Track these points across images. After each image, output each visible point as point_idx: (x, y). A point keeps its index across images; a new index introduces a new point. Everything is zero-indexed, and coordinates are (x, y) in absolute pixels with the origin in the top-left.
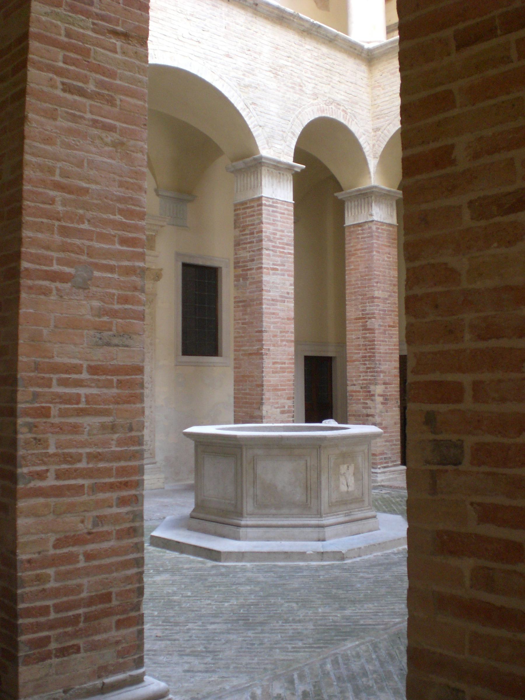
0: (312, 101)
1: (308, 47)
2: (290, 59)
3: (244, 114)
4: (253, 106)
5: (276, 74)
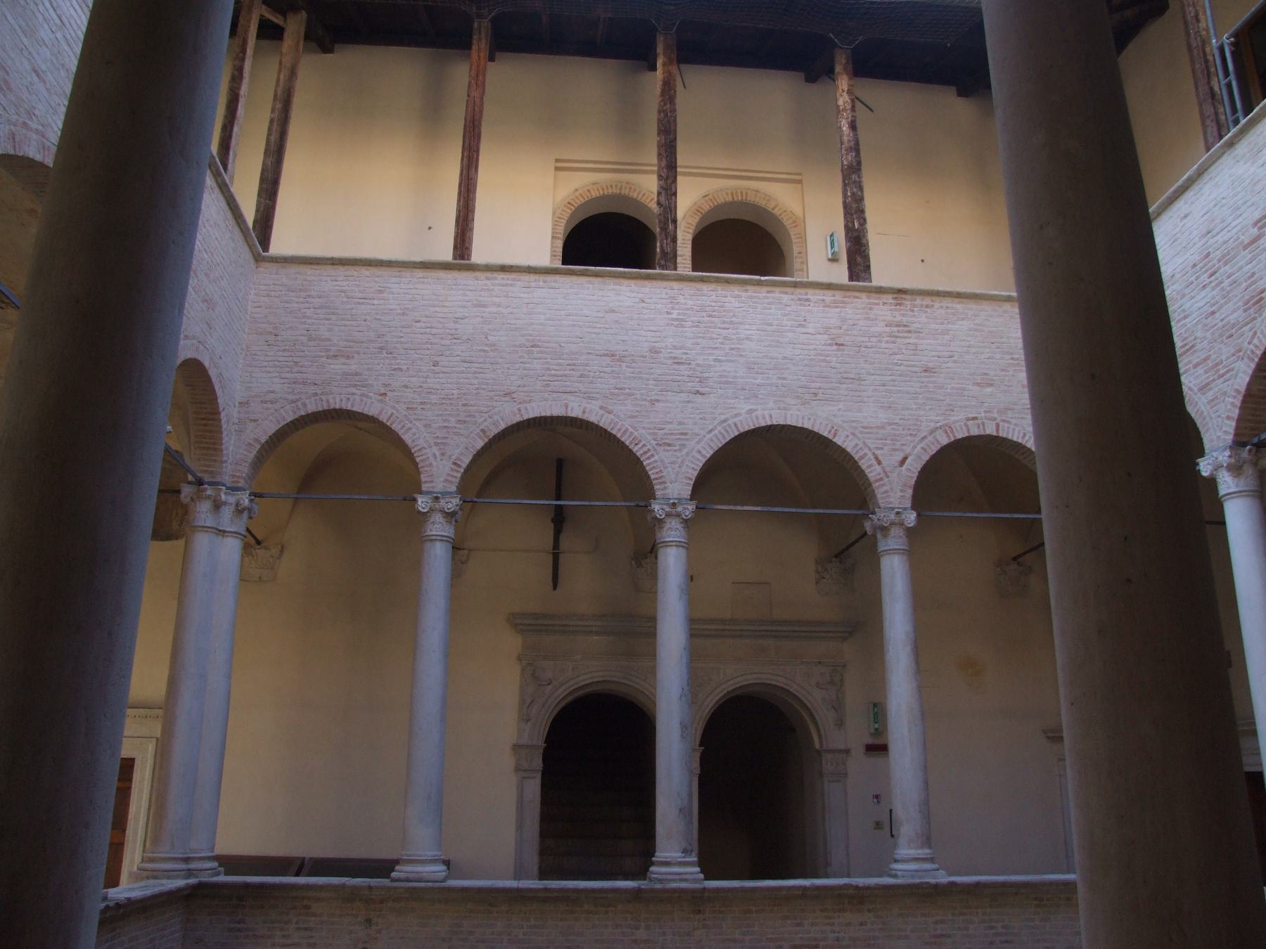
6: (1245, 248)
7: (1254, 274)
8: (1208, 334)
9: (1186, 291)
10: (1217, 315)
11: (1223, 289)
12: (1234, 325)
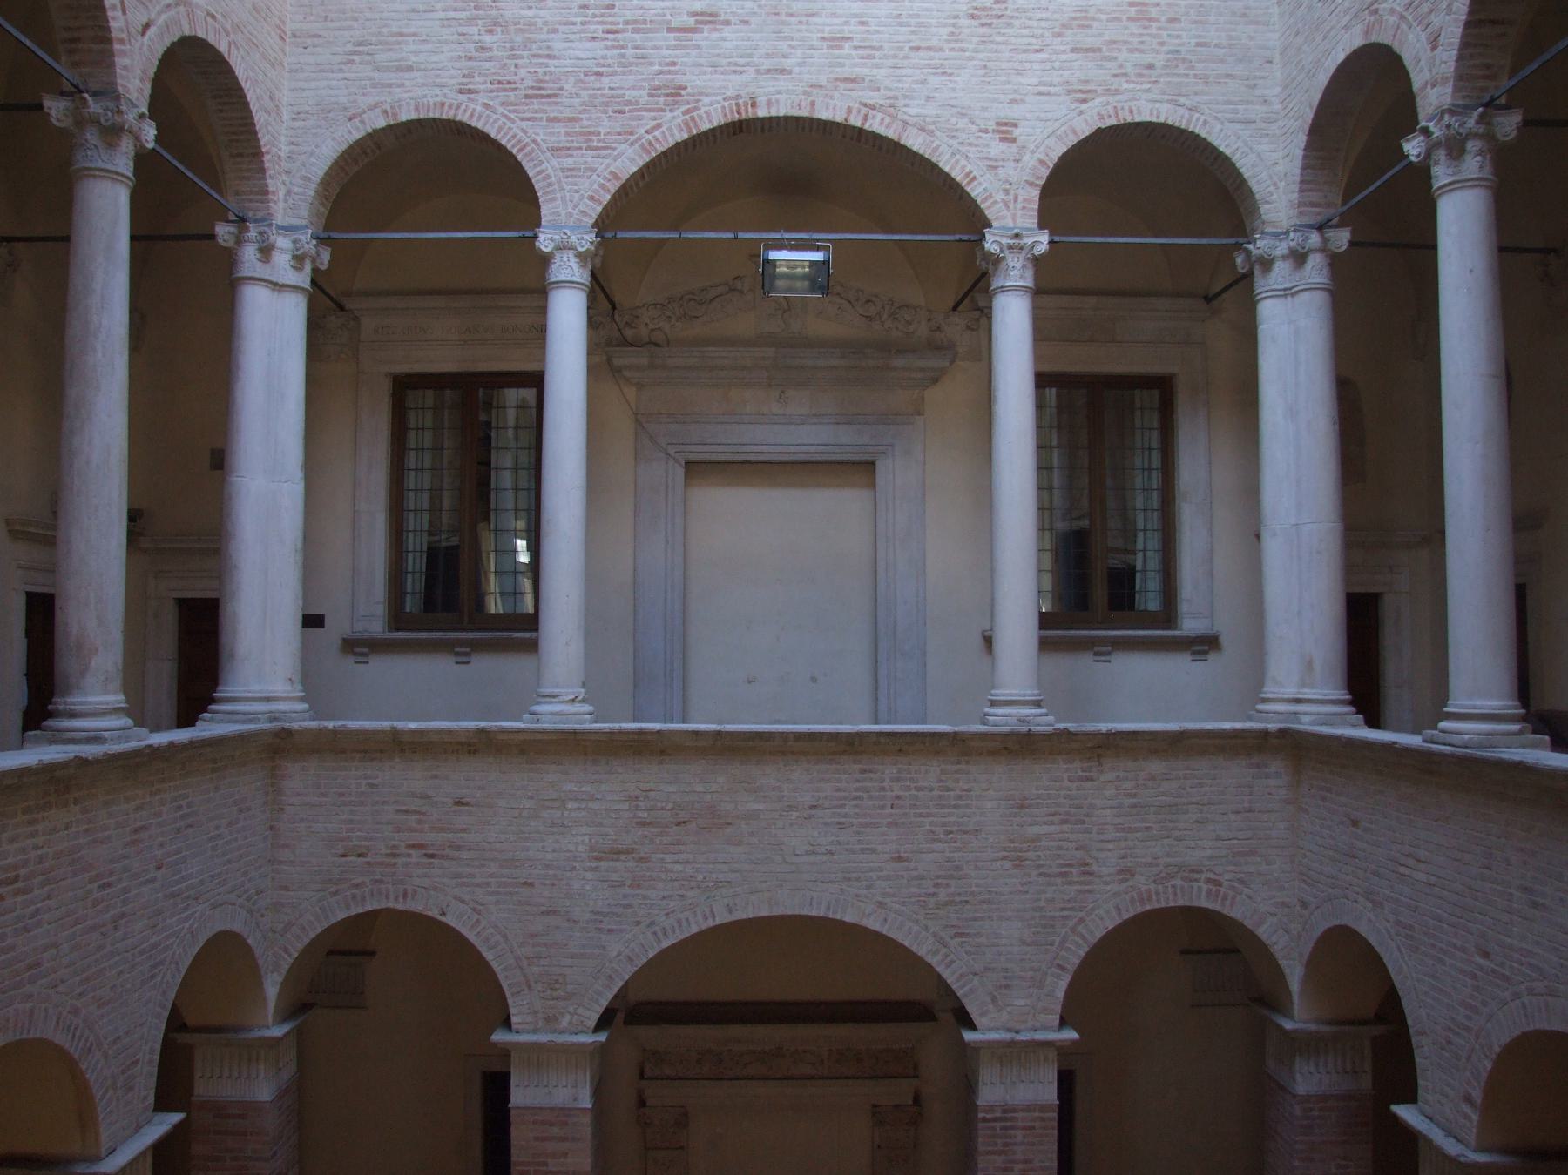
0: (1116, 888)
1: (1110, 776)
2: (1056, 819)
3: (933, 960)
4: (958, 940)
5: (1020, 858)
6: (670, 30)
7: (674, 64)
8: (584, 94)
9: (562, 28)
10: (605, 80)
11: (623, 56)
12: (629, 103)
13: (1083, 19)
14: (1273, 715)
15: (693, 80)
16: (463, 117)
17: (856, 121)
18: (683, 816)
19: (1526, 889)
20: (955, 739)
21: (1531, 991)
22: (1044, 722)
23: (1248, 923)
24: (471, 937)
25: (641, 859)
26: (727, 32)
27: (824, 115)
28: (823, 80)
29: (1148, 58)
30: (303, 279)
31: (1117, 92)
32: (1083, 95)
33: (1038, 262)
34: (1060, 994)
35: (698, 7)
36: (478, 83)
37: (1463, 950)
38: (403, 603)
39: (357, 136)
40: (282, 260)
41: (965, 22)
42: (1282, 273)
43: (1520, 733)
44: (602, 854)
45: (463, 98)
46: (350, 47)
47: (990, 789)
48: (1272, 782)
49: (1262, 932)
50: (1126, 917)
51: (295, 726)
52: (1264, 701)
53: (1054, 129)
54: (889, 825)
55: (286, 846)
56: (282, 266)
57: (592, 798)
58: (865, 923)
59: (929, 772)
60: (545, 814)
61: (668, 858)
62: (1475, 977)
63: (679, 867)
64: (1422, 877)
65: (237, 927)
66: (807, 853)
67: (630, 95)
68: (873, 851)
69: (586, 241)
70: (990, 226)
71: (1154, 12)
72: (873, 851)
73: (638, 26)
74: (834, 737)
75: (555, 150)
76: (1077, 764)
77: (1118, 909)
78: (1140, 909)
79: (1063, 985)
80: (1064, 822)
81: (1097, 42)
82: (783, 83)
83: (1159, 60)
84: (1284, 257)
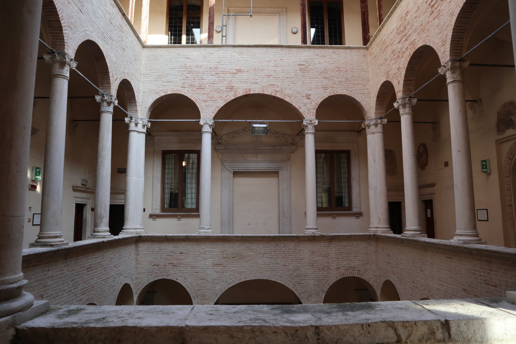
3: (293, 290)
12: (221, 90)
13: (326, 71)
14: (372, 231)
15: (236, 85)
16: (182, 93)
17: (273, 94)
18: (234, 256)
19: (420, 267)
20: (297, 237)
21: (421, 290)
22: (318, 233)
23: (367, 280)
24: (184, 285)
25: (224, 266)
26: (244, 74)
27: (266, 93)
28: (266, 85)
29: (340, 80)
30: (145, 130)
31: (334, 87)
32: (325, 88)
33: (315, 127)
34: (323, 298)
35: (237, 68)
36: (186, 85)
37: (409, 282)
38: (164, 205)
39: (158, 97)
40: (140, 126)
41: (298, 71)
42: (373, 129)
43: (421, 234)
44: (214, 265)
45: (183, 89)
46: (156, 77)
47: (306, 249)
48: (372, 247)
49: (370, 282)
50: (338, 279)
51: (142, 235)
52: (370, 228)
53: (319, 96)
54: (282, 258)
55: (139, 264)
56: (140, 128)
57: (213, 252)
58: (277, 281)
59: (291, 245)
60: (201, 256)
61: (230, 266)
62: (412, 288)
63: (233, 268)
64: (402, 267)
65: (129, 283)
66: (263, 264)
67: (221, 88)
68: (279, 264)
69: (211, 122)
70: (304, 119)
71: (342, 69)
72: (279, 264)
73: (223, 72)
74: (270, 237)
75: (204, 101)
76: (326, 243)
77: (336, 277)
78: (341, 277)
79: (324, 295)
80: (323, 257)
81: (329, 76)
82: (256, 86)
83: (343, 80)
84: (372, 125)
